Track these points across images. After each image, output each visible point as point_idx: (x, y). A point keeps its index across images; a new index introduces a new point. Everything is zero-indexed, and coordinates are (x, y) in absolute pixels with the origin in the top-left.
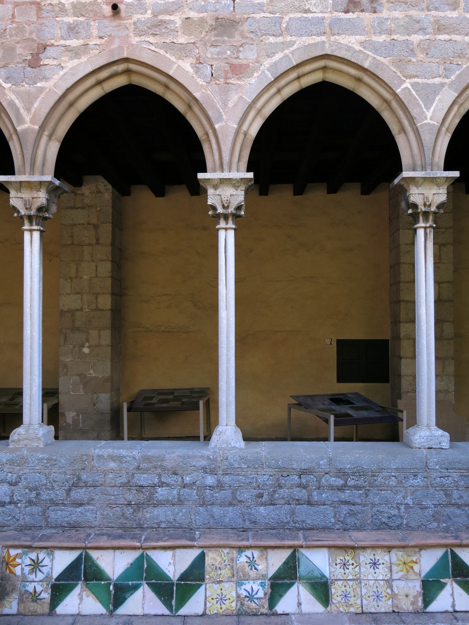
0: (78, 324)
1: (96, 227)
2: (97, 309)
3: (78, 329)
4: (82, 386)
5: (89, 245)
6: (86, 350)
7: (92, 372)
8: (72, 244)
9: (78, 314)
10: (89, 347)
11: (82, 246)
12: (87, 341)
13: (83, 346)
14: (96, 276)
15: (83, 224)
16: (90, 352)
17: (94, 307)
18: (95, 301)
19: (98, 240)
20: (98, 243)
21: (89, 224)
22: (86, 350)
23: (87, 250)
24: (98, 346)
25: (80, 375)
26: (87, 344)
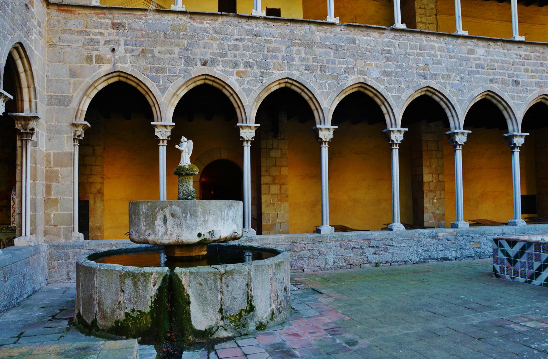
0: (431, 188)
1: (437, 142)
2: (439, 181)
3: (431, 191)
4: (434, 218)
5: (434, 151)
6: (435, 201)
7: (437, 211)
8: (427, 150)
9: (431, 183)
10: (436, 199)
11: (432, 151)
12: (435, 196)
13: (433, 199)
14: (438, 165)
15: (431, 141)
16: (437, 201)
17: (438, 180)
18: (438, 177)
19: (438, 148)
20: (438, 150)
21: (434, 140)
22: (435, 201)
23: (434, 153)
24: (440, 198)
25: (433, 213)
26: (435, 198)
